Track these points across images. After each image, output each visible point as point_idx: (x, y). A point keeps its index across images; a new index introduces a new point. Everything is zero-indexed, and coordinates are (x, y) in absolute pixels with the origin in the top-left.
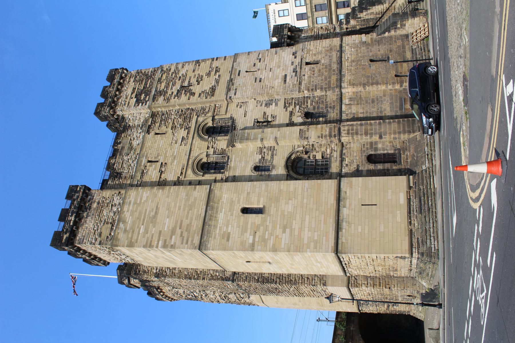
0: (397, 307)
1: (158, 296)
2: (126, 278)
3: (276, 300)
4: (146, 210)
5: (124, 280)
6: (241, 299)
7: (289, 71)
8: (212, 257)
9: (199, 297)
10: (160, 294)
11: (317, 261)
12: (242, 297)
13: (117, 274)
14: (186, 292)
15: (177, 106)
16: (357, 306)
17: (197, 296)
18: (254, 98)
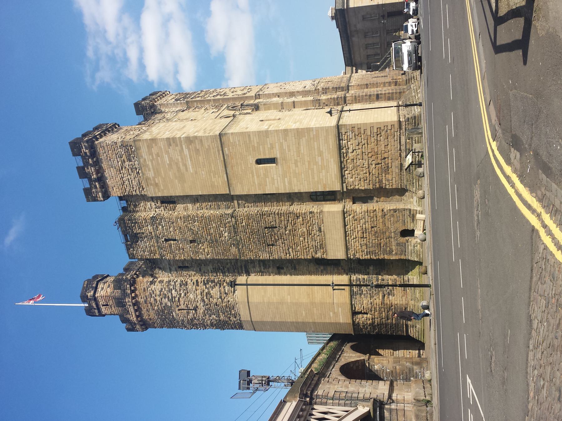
0: (393, 297)
1: (127, 300)
2: (92, 290)
3: (263, 294)
4: (174, 127)
5: (88, 292)
6: (225, 295)
7: (308, 85)
8: (227, 153)
9: (177, 299)
10: (131, 294)
11: (319, 148)
12: (227, 292)
13: (84, 285)
14: (163, 290)
15: (212, 101)
16: (350, 296)
17: (174, 297)
18: (278, 94)
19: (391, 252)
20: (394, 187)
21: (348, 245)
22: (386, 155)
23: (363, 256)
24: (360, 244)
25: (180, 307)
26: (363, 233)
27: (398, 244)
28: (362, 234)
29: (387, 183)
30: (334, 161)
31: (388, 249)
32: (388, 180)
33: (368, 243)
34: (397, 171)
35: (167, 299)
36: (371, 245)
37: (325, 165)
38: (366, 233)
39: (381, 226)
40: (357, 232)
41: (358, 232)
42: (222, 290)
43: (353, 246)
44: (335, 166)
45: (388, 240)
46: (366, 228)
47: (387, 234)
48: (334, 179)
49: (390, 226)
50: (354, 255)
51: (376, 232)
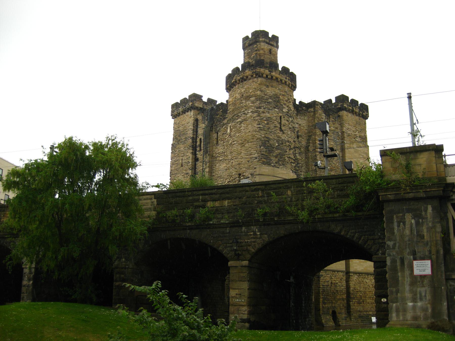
19: (324, 303)
20: (352, 307)
21: (328, 272)
22: (365, 302)
23: (322, 283)
24: (329, 281)
25: (282, 119)
26: (334, 284)
27: (328, 309)
28: (334, 283)
29: (353, 302)
30: (363, 270)
31: (326, 302)
32: (354, 303)
33: (329, 287)
34: (358, 309)
35: (287, 111)
36: (328, 289)
37: (361, 264)
38: (335, 286)
39: (338, 297)
40: (335, 279)
41: (334, 280)
42: (293, 161)
43: (327, 276)
44: (360, 270)
45: (331, 301)
46: (337, 286)
47: (334, 301)
48: (355, 268)
49: (338, 303)
50: (322, 276)
51: (335, 294)
